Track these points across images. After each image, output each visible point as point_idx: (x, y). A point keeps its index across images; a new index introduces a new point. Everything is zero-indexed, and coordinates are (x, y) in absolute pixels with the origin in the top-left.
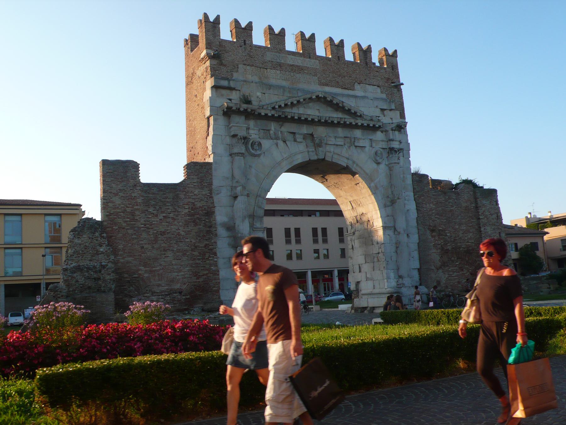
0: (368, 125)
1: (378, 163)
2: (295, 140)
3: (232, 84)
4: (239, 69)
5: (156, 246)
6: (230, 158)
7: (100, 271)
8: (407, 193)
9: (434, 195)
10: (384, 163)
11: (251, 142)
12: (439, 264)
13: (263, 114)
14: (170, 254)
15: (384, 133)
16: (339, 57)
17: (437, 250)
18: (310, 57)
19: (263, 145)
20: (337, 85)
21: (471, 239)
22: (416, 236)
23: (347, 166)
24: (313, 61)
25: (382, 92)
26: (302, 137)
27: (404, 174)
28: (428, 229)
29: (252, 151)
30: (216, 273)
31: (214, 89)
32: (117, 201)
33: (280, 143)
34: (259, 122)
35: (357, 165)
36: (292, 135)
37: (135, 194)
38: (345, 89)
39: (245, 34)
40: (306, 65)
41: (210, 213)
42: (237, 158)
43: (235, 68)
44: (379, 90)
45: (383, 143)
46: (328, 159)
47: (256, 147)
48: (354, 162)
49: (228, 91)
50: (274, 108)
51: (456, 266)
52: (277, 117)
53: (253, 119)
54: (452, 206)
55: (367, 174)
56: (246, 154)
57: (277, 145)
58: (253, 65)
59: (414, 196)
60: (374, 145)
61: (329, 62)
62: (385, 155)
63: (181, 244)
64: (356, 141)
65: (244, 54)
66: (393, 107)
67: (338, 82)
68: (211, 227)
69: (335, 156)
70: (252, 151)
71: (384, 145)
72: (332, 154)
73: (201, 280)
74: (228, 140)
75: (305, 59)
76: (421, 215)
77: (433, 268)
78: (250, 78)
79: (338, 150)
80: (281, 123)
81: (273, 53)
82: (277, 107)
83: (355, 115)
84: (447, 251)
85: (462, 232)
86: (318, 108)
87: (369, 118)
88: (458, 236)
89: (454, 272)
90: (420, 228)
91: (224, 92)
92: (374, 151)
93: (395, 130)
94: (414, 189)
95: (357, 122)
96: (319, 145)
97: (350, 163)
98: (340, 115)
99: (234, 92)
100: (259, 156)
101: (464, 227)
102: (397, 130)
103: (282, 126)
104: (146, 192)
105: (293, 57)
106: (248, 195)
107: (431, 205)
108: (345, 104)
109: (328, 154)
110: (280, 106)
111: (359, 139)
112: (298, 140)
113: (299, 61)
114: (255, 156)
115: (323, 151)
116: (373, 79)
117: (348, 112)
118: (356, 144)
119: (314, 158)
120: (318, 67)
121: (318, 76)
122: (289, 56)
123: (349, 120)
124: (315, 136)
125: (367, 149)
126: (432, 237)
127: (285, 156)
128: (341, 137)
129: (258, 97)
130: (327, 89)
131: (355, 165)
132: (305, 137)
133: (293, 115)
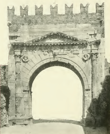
1: (85, 61)
11: (23, 56)
23: (69, 63)
26: (47, 52)
29: (24, 60)
47: (25, 58)
83: (73, 39)
100: (27, 62)
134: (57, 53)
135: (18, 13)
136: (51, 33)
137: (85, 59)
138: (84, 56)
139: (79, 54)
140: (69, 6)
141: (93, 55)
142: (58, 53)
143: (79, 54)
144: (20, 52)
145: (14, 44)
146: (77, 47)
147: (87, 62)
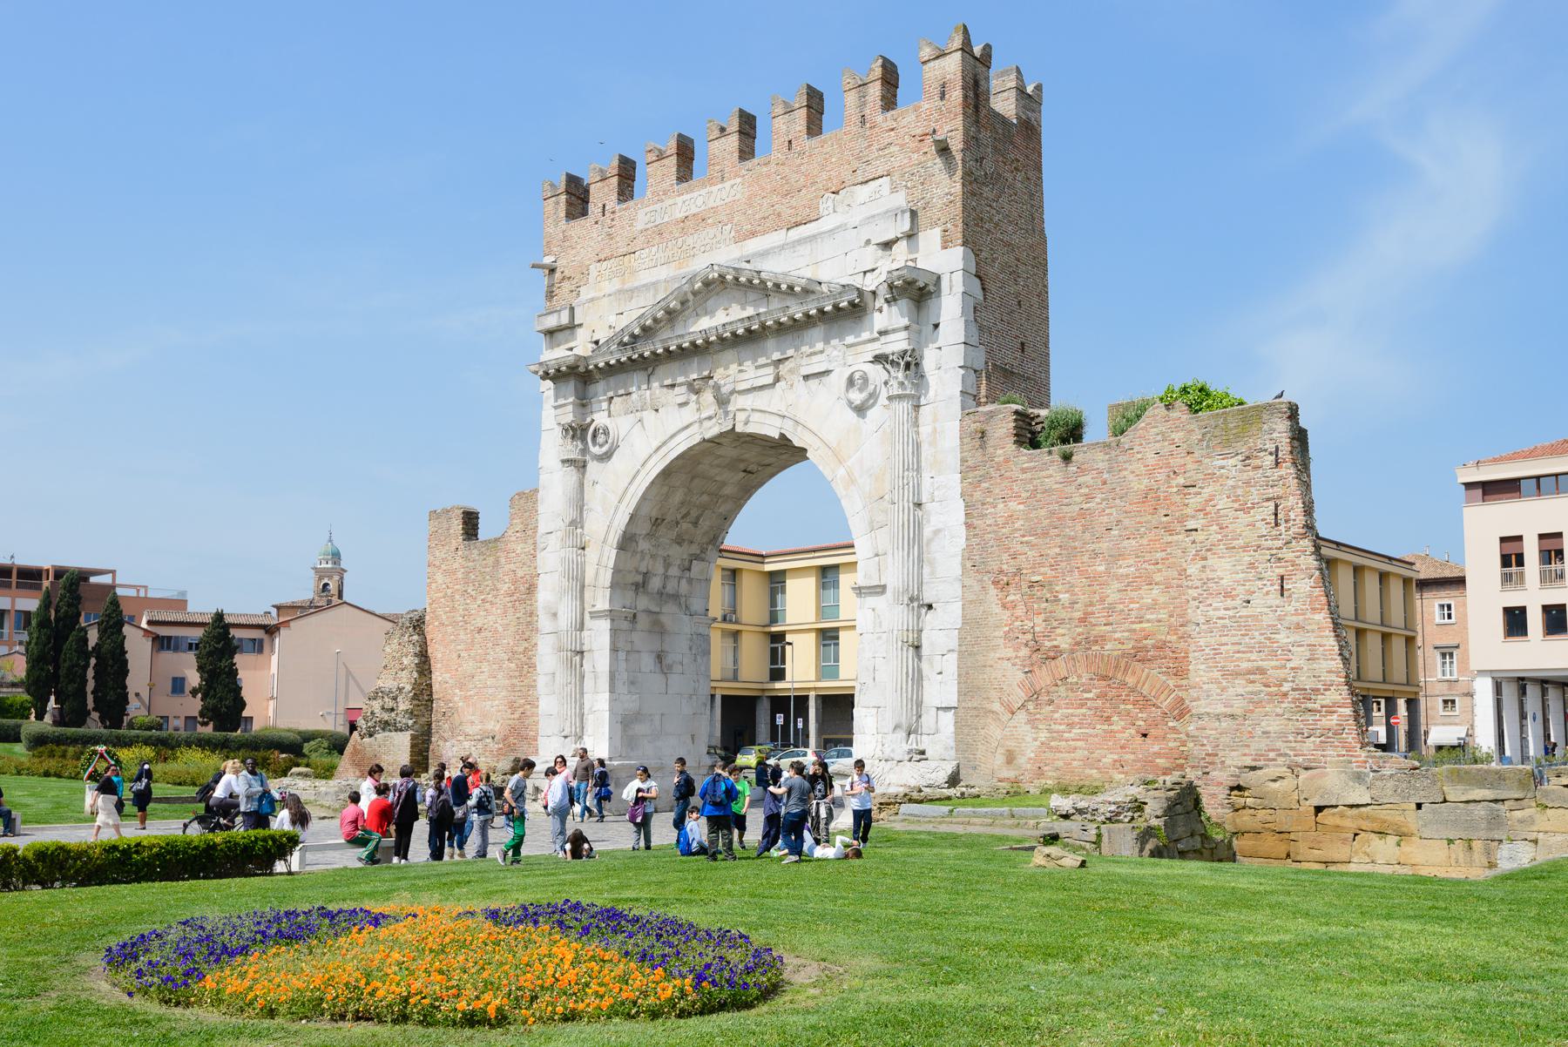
1: (861, 410)
5: (472, 653)
7: (395, 699)
9: (1024, 471)
12: (1019, 696)
13: (601, 365)
14: (485, 667)
17: (1017, 649)
21: (1153, 607)
22: (957, 608)
24: (728, 184)
25: (894, 190)
26: (684, 389)
27: (935, 420)
28: (995, 583)
30: (534, 704)
32: (439, 578)
33: (648, 415)
37: (456, 565)
40: (711, 204)
41: (531, 589)
43: (585, 273)
49: (567, 332)
50: (622, 344)
51: (1082, 706)
54: (1089, 498)
59: (963, 479)
63: (498, 649)
68: (531, 614)
69: (756, 417)
73: (516, 716)
76: (975, 541)
77: (996, 706)
84: (1054, 655)
85: (1116, 585)
88: (1102, 600)
89: (1071, 725)
90: (968, 582)
91: (560, 336)
94: (963, 460)
95: (791, 311)
98: (776, 303)
100: (606, 457)
101: (1126, 568)
104: (466, 558)
107: (1013, 505)
109: (741, 417)
119: (712, 430)
126: (1004, 606)
127: (655, 444)
130: (753, 245)
136: (691, 281)
137: (857, 397)
138: (851, 382)
139: (827, 372)
143: (827, 372)
144: (570, 408)
146: (817, 332)
147: (870, 413)
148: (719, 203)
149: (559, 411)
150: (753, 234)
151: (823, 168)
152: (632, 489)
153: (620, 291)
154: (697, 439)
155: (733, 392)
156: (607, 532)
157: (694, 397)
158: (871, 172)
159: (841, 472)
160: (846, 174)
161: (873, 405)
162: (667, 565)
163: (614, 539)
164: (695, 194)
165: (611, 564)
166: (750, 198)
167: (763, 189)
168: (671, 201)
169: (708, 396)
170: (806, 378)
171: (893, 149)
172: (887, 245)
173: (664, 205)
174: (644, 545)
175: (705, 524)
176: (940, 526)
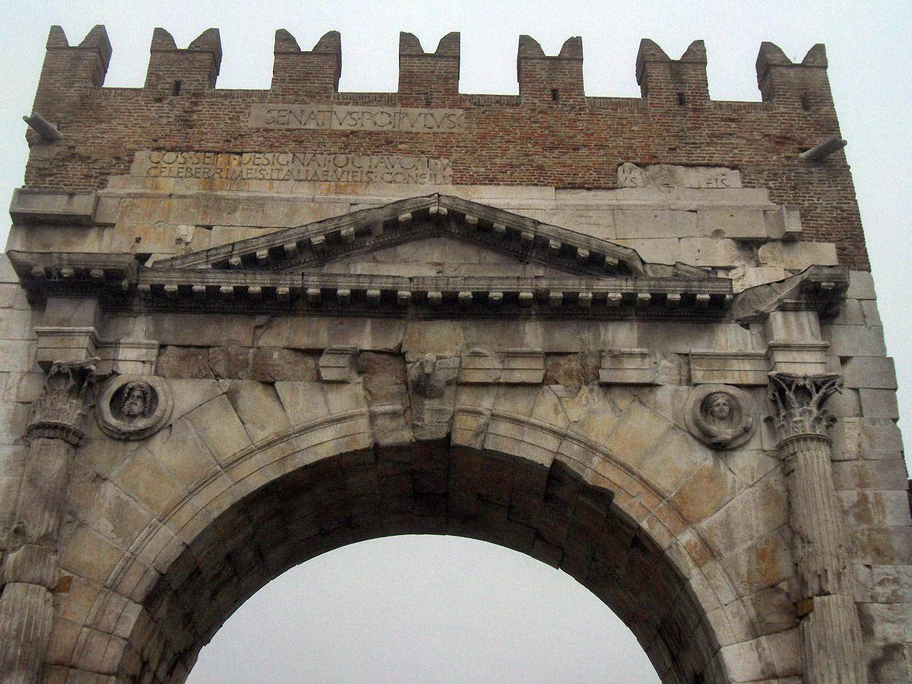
0: (659, 299)
1: (720, 448)
2: (319, 379)
3: (82, 205)
4: (134, 168)
6: (20, 448)
8: (889, 569)
10: (754, 444)
11: (115, 385)
15: (755, 329)
16: (555, 94)
18: (428, 105)
19: (162, 398)
20: (538, 178)
23: (555, 462)
24: (439, 113)
25: (747, 184)
26: (343, 361)
27: (862, 484)
29: (113, 421)
31: (21, 232)
34: (168, 322)
35: (608, 457)
36: (311, 362)
38: (573, 187)
39: (185, 65)
40: (405, 126)
42: (37, 443)
43: (123, 161)
44: (734, 178)
45: (747, 365)
46: (464, 435)
48: (591, 448)
52: (227, 296)
53: (148, 313)
55: (660, 495)
56: (94, 432)
57: (232, 396)
58: (189, 149)
60: (698, 375)
61: (509, 111)
62: (755, 409)
64: (607, 363)
65: (164, 121)
66: (793, 224)
67: (541, 168)
69: (503, 428)
70: (113, 421)
71: (749, 373)
72: (482, 420)
74: (32, 389)
75: (409, 110)
78: (169, 185)
79: (517, 406)
80: (261, 320)
81: (280, 106)
82: (235, 260)
86: (436, 258)
87: (669, 272)
92: (692, 397)
93: (796, 309)
96: (421, 388)
97: (572, 454)
99: (93, 233)
100: (143, 436)
102: (809, 308)
103: (268, 325)
105: (356, 109)
106: (58, 589)
108: (543, 230)
110: (250, 262)
111: (618, 356)
112: (326, 375)
113: (380, 120)
114: (126, 438)
115: (440, 411)
116: (708, 144)
117: (566, 256)
118: (605, 376)
120: (455, 130)
121: (454, 157)
122: (341, 110)
123: (560, 284)
124: (409, 357)
125: (663, 395)
127: (261, 436)
128: (532, 355)
129: (179, 241)
131: (596, 460)
132: (361, 362)
133: (298, 282)
134: (441, 376)
135: (128, 69)
137: (724, 431)
138: (706, 405)
140: (552, 48)
141: (790, 394)
142: (453, 375)
143: (652, 386)
144: (85, 341)
145: (39, 269)
148: (419, 127)
149: (44, 342)
150: (492, 181)
151: (616, 133)
152: (198, 501)
153: (207, 198)
154: (364, 442)
155: (449, 383)
156: (124, 570)
157: (360, 379)
158: (698, 155)
159: (687, 537)
160: (663, 153)
161: (741, 446)
162: (162, 658)
163: (138, 583)
164: (374, 110)
165: (126, 629)
166: (483, 137)
167: (508, 132)
168: (322, 107)
169: (386, 380)
170: (607, 387)
171: (732, 141)
172: (748, 245)
173: (308, 108)
174: (162, 611)
175: (220, 599)
176: (894, 639)
